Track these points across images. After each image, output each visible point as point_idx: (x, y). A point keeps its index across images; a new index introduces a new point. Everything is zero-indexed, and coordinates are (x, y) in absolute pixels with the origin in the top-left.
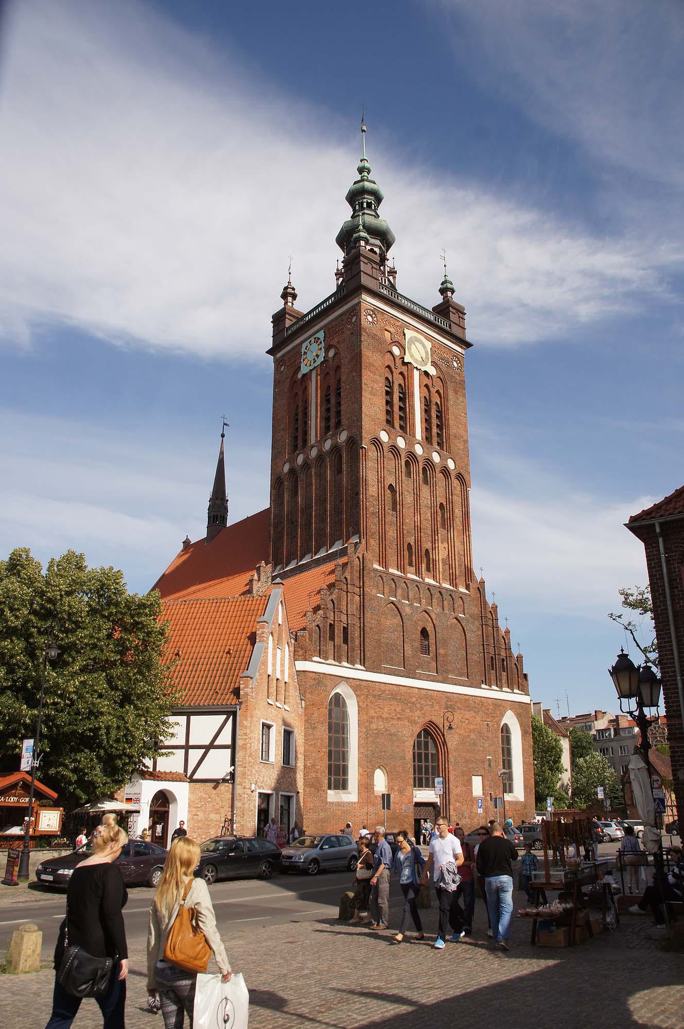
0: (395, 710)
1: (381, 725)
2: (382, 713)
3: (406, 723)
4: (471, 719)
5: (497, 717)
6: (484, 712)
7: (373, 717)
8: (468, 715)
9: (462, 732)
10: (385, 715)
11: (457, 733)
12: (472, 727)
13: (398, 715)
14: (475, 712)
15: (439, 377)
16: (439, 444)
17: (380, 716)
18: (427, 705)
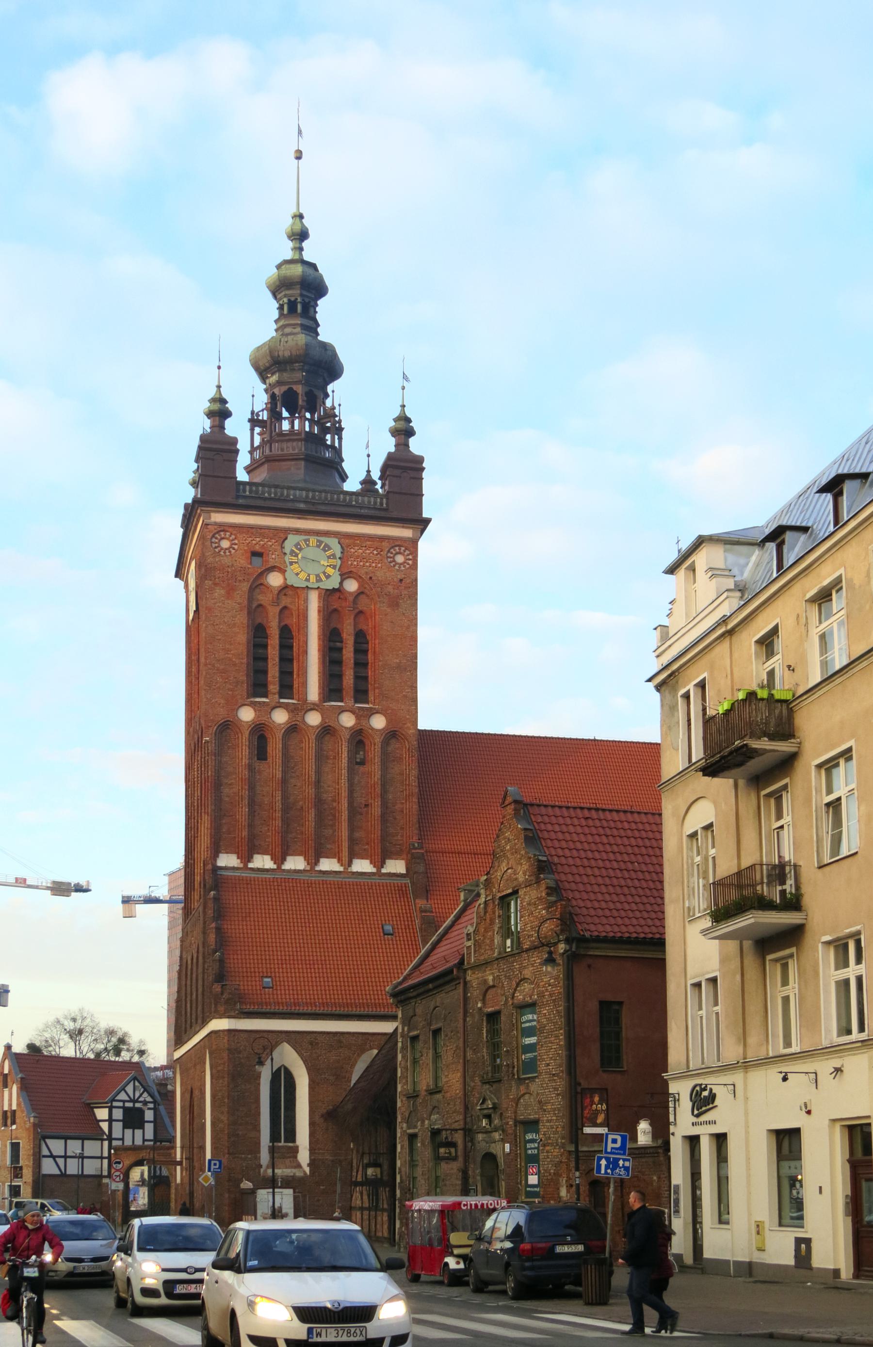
15: (363, 593)
16: (361, 694)
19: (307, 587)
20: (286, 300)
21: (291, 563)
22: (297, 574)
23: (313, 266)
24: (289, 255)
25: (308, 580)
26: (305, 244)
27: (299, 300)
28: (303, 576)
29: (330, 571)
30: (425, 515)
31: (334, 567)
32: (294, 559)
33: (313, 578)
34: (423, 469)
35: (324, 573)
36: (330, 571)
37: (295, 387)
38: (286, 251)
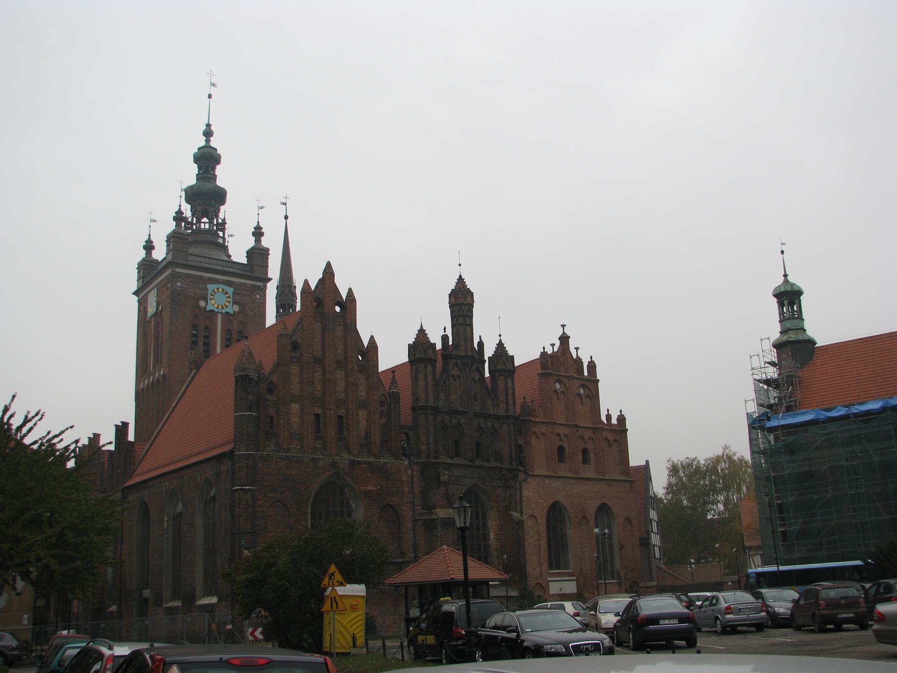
20: (203, 165)
21: (211, 299)
22: (213, 305)
23: (216, 150)
24: (203, 144)
25: (218, 308)
26: (211, 139)
27: (210, 165)
28: (216, 305)
29: (227, 304)
30: (269, 276)
31: (229, 302)
32: (212, 297)
33: (220, 307)
34: (269, 254)
35: (225, 305)
36: (227, 304)
37: (207, 208)
38: (202, 142)
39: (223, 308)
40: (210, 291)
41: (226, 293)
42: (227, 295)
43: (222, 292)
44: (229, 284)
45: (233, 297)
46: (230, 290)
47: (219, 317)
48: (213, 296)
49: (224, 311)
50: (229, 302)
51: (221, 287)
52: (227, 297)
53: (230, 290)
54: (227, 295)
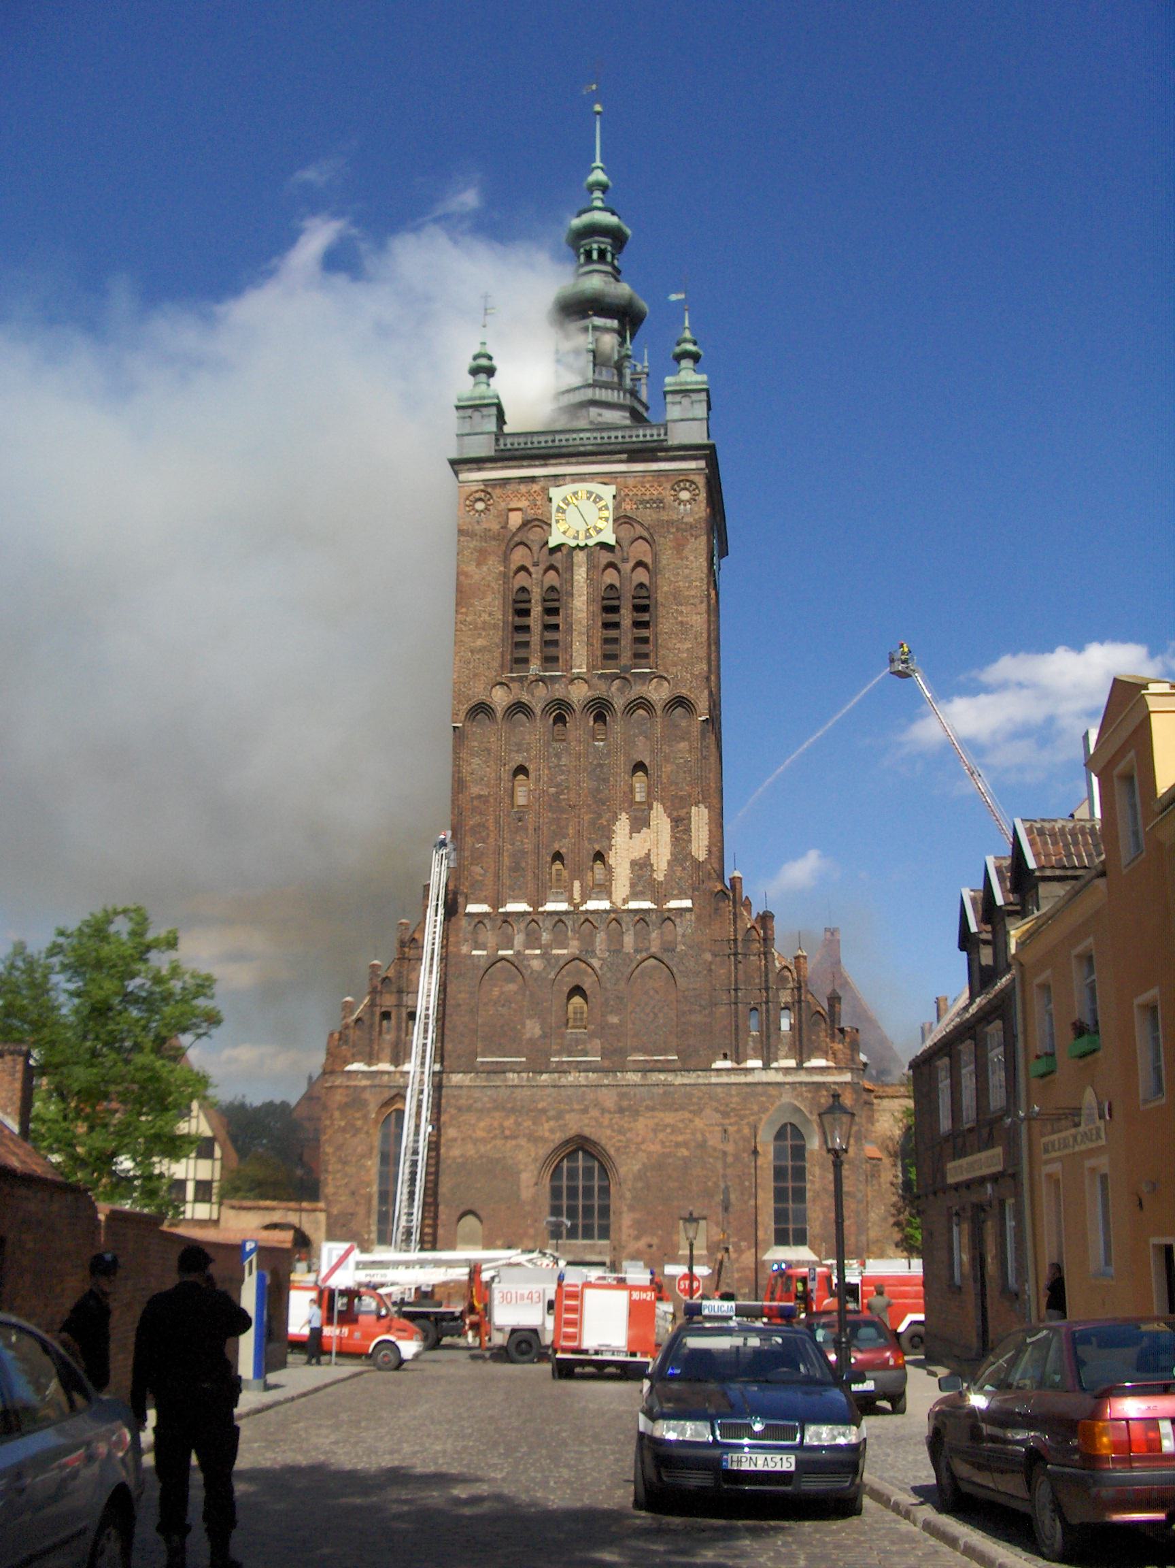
0: (501, 1126)
1: (471, 1150)
2: (474, 1131)
3: (522, 1141)
4: (681, 1125)
5: (752, 1114)
6: (717, 1110)
7: (455, 1140)
8: (669, 1118)
9: (652, 1148)
10: (480, 1134)
11: (644, 1151)
12: (680, 1138)
13: (507, 1133)
14: (691, 1112)
17: (471, 1137)
18: (573, 1110)
19: (578, 545)
21: (557, 521)
27: (595, 246)
28: (571, 533)
31: (607, 519)
33: (581, 536)
36: (601, 524)
39: (591, 536)
40: (557, 501)
41: (599, 498)
42: (602, 503)
43: (588, 498)
44: (606, 479)
45: (616, 508)
46: (608, 492)
47: (580, 557)
48: (564, 512)
49: (591, 542)
50: (607, 519)
51: (582, 487)
52: (600, 509)
53: (608, 492)
54: (602, 503)
